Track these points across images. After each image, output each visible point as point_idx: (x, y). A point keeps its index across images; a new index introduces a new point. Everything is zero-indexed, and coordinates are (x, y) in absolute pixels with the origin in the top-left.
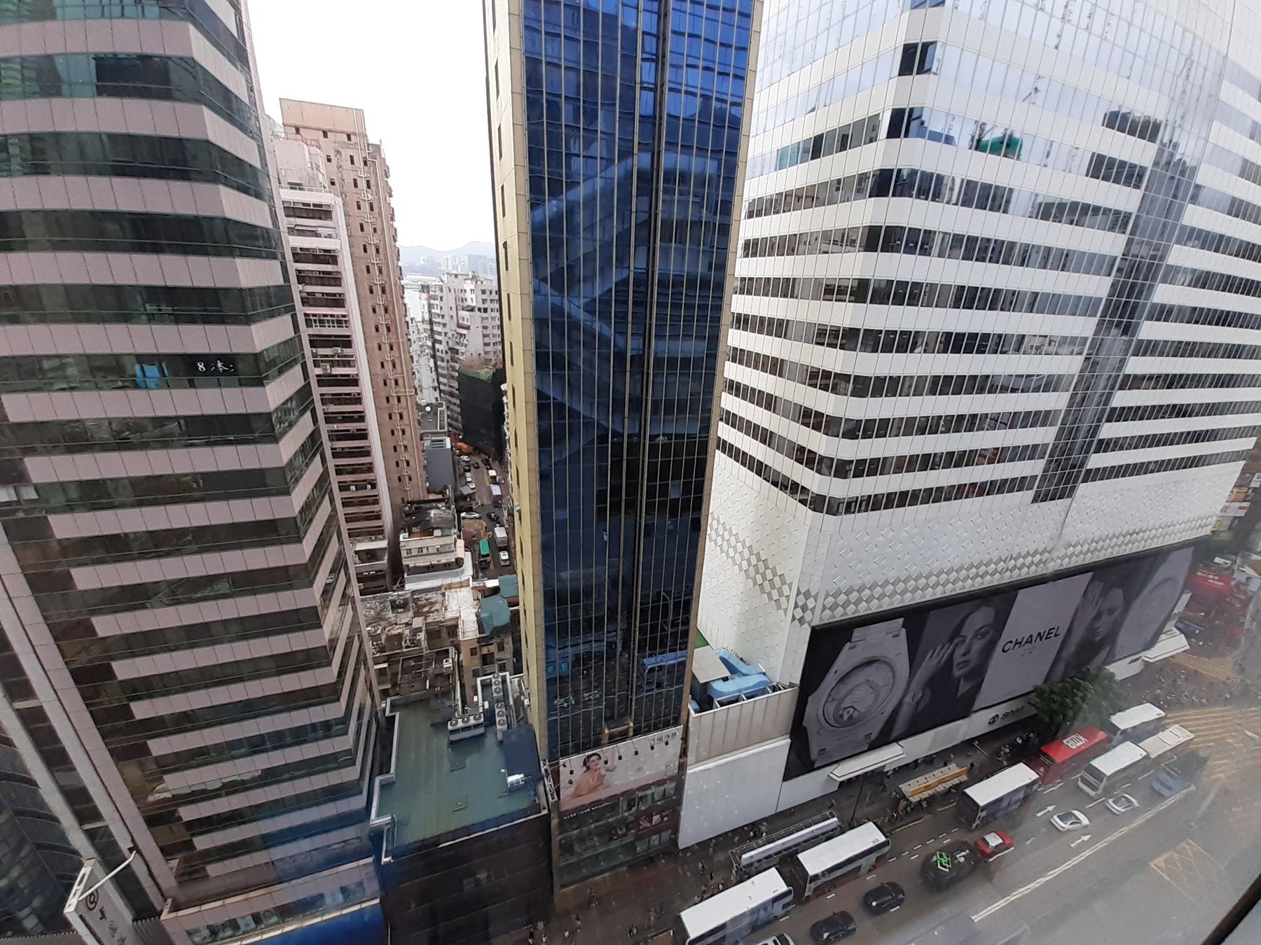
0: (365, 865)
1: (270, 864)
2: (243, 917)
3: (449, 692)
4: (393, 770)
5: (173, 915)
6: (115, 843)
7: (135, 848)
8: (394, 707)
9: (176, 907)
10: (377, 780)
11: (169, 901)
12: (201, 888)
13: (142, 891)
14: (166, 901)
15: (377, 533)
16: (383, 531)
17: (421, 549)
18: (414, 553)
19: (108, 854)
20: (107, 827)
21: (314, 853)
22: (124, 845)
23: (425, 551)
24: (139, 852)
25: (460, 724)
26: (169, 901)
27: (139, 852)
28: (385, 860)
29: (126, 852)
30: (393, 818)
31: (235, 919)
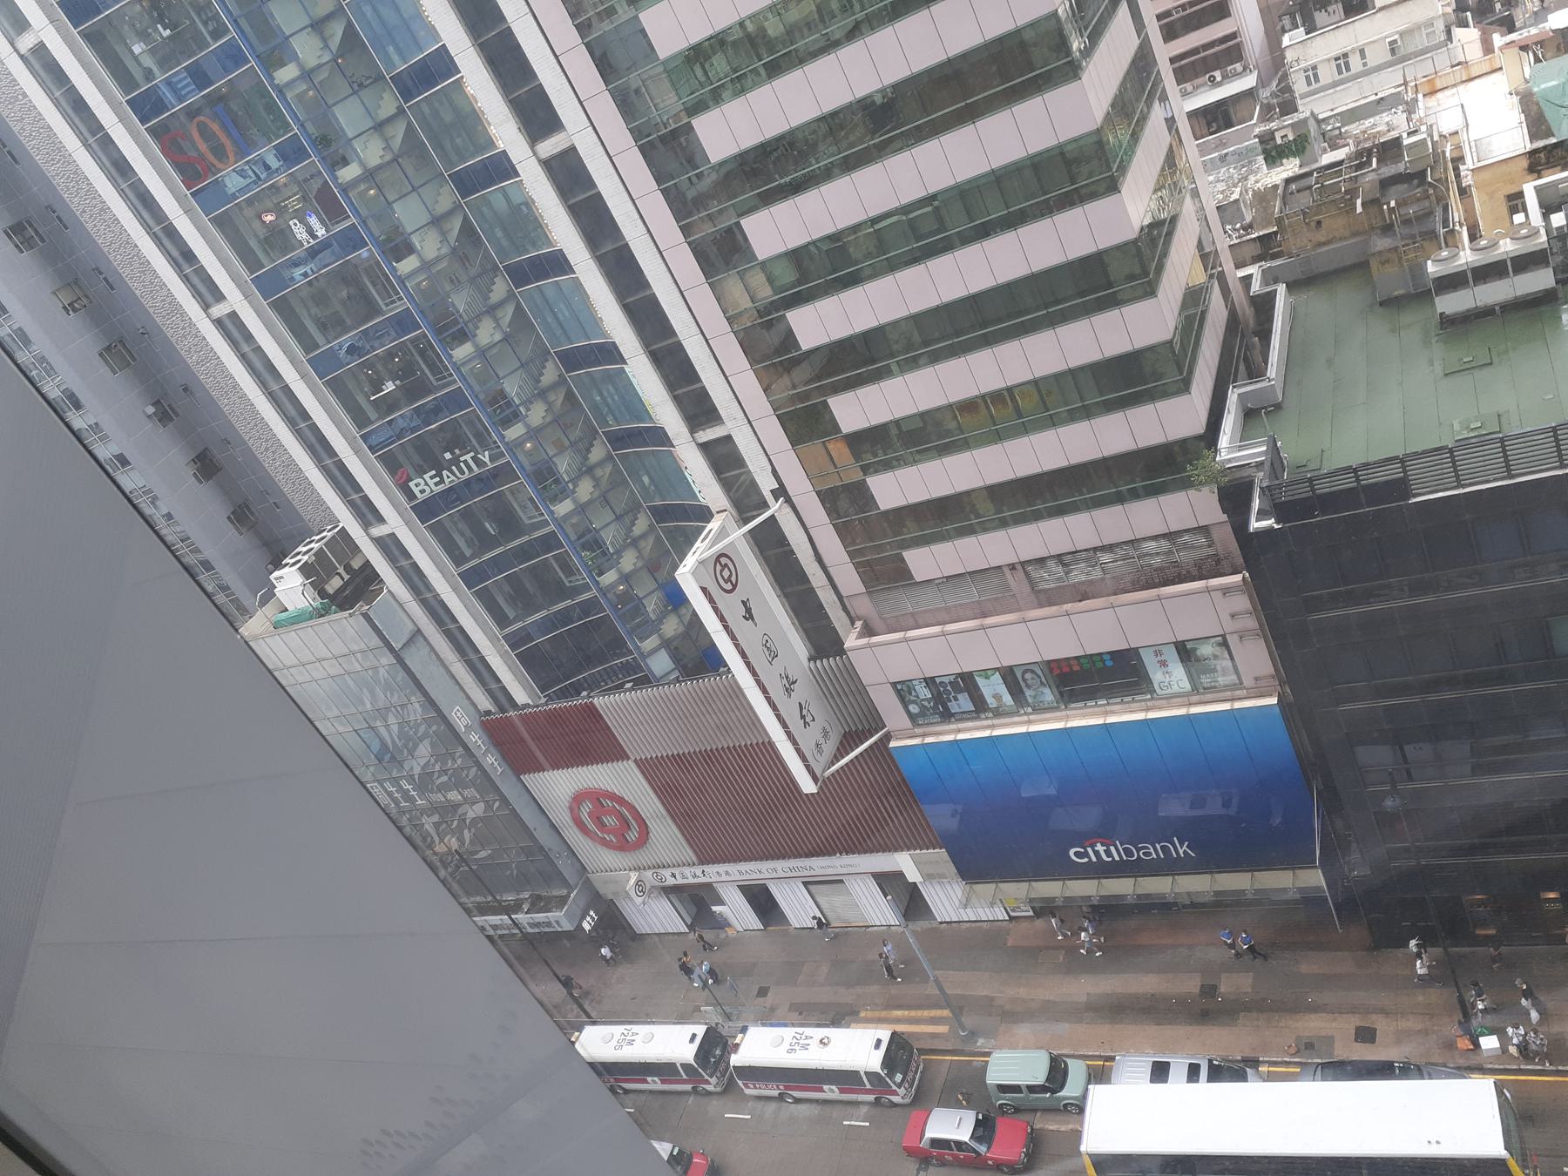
0: (1226, 591)
1: (1019, 567)
2: (985, 673)
3: (1430, 213)
4: (1272, 371)
5: (864, 641)
6: (754, 484)
7: (781, 492)
8: (1270, 277)
9: (868, 631)
10: (1233, 397)
11: (859, 624)
12: (906, 602)
13: (803, 578)
14: (853, 623)
15: (1228, 54)
16: (1238, 47)
17: (1342, 61)
18: (1327, 74)
19: (746, 500)
20: (729, 438)
21: (1105, 558)
22: (766, 484)
23: (1356, 63)
24: (789, 501)
25: (1467, 257)
26: (859, 624)
27: (789, 501)
28: (1255, 525)
29: (769, 498)
30: (1274, 450)
31: (971, 673)
